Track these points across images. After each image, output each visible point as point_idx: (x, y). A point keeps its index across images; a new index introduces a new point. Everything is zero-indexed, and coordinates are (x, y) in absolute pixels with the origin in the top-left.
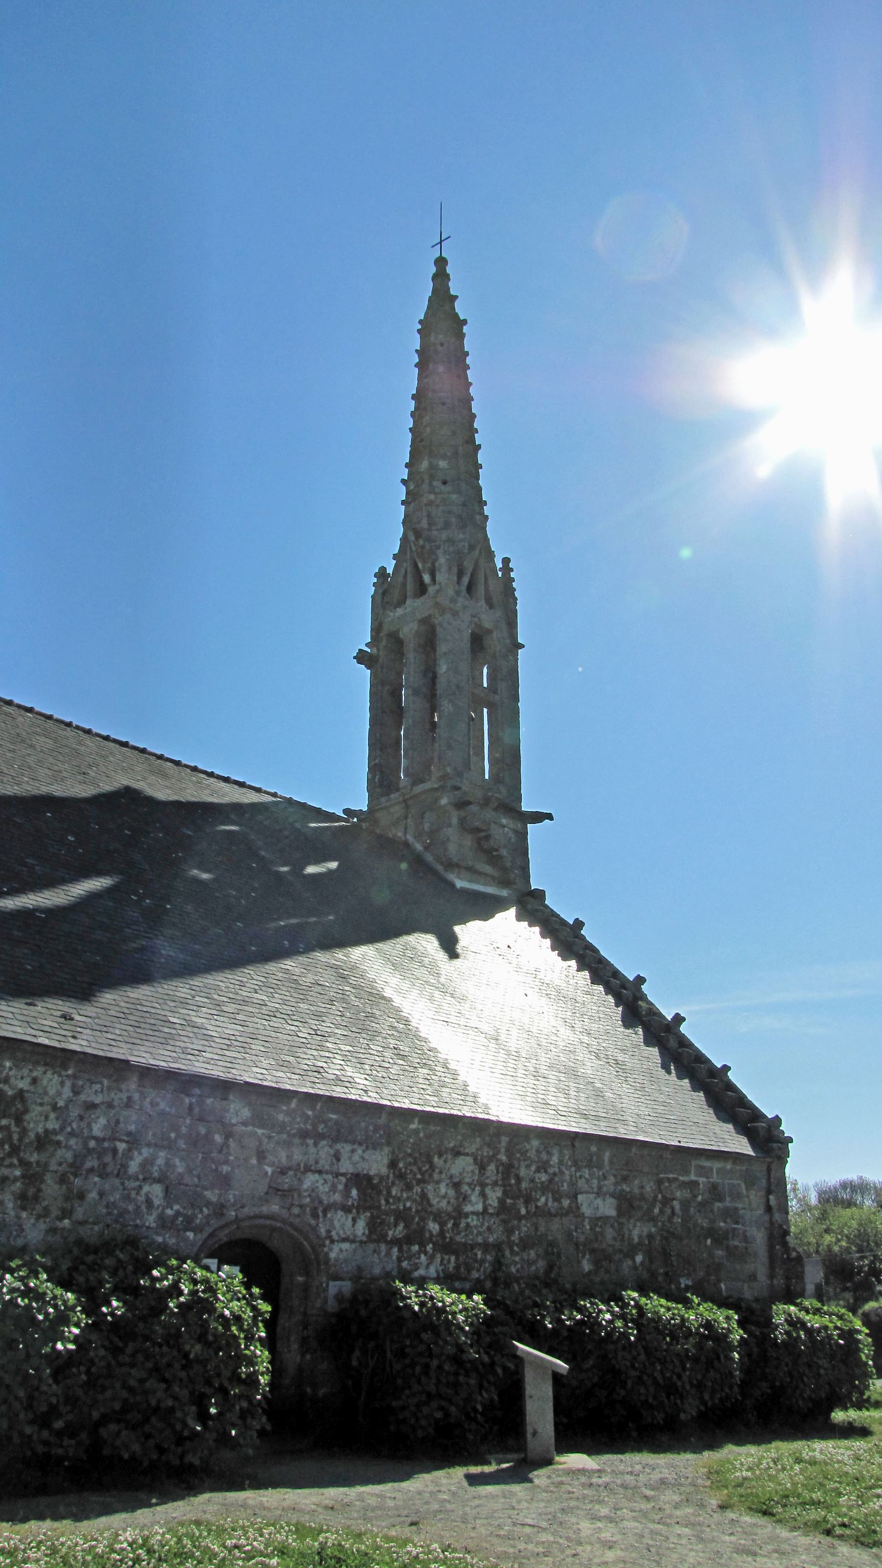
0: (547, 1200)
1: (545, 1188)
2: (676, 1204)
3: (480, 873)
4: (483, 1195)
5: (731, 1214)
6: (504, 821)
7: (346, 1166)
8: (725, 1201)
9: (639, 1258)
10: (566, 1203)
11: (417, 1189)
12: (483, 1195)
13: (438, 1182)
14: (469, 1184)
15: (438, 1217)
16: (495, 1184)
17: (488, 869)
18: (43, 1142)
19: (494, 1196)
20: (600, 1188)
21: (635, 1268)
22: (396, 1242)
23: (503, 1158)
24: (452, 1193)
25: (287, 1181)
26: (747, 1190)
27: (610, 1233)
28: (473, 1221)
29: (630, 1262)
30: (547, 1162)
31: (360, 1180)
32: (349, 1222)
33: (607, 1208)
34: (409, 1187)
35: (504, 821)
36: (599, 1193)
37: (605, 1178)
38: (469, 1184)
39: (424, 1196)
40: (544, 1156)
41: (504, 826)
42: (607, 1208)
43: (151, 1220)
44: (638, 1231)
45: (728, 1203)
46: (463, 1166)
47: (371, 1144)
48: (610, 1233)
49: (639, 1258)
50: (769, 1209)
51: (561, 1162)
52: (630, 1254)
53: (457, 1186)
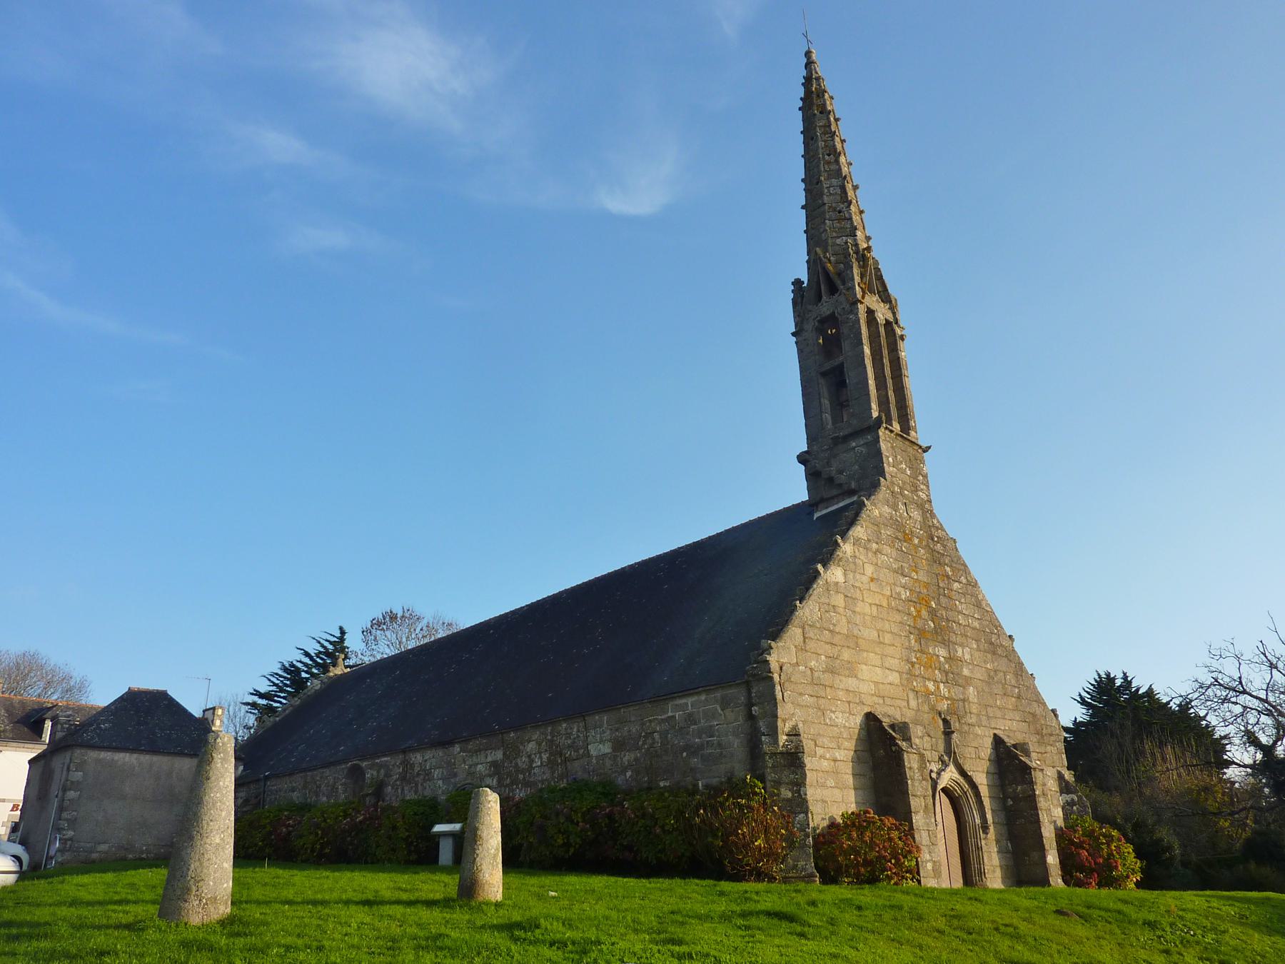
0: (571, 753)
1: (569, 747)
2: (656, 736)
3: (833, 498)
4: (541, 758)
5: (710, 732)
6: (854, 444)
7: (489, 759)
8: (700, 722)
9: (629, 774)
10: (581, 751)
11: (514, 762)
12: (541, 758)
13: (522, 757)
14: (535, 754)
15: (523, 772)
16: (546, 751)
17: (835, 492)
18: (418, 774)
19: (545, 757)
20: (601, 738)
21: (627, 780)
22: (507, 785)
23: (549, 737)
24: (527, 760)
25: (473, 769)
26: (722, 710)
27: (608, 763)
28: (536, 771)
29: (623, 777)
30: (571, 733)
31: (494, 764)
32: (491, 781)
33: (606, 749)
34: (511, 762)
35: (854, 444)
36: (601, 741)
37: (604, 732)
38: (535, 754)
39: (517, 764)
40: (569, 731)
41: (854, 448)
42: (606, 749)
43: (440, 791)
44: (628, 757)
45: (703, 723)
46: (531, 746)
47: (495, 749)
48: (608, 763)
49: (629, 774)
50: (751, 717)
51: (578, 731)
52: (624, 770)
53: (529, 756)
